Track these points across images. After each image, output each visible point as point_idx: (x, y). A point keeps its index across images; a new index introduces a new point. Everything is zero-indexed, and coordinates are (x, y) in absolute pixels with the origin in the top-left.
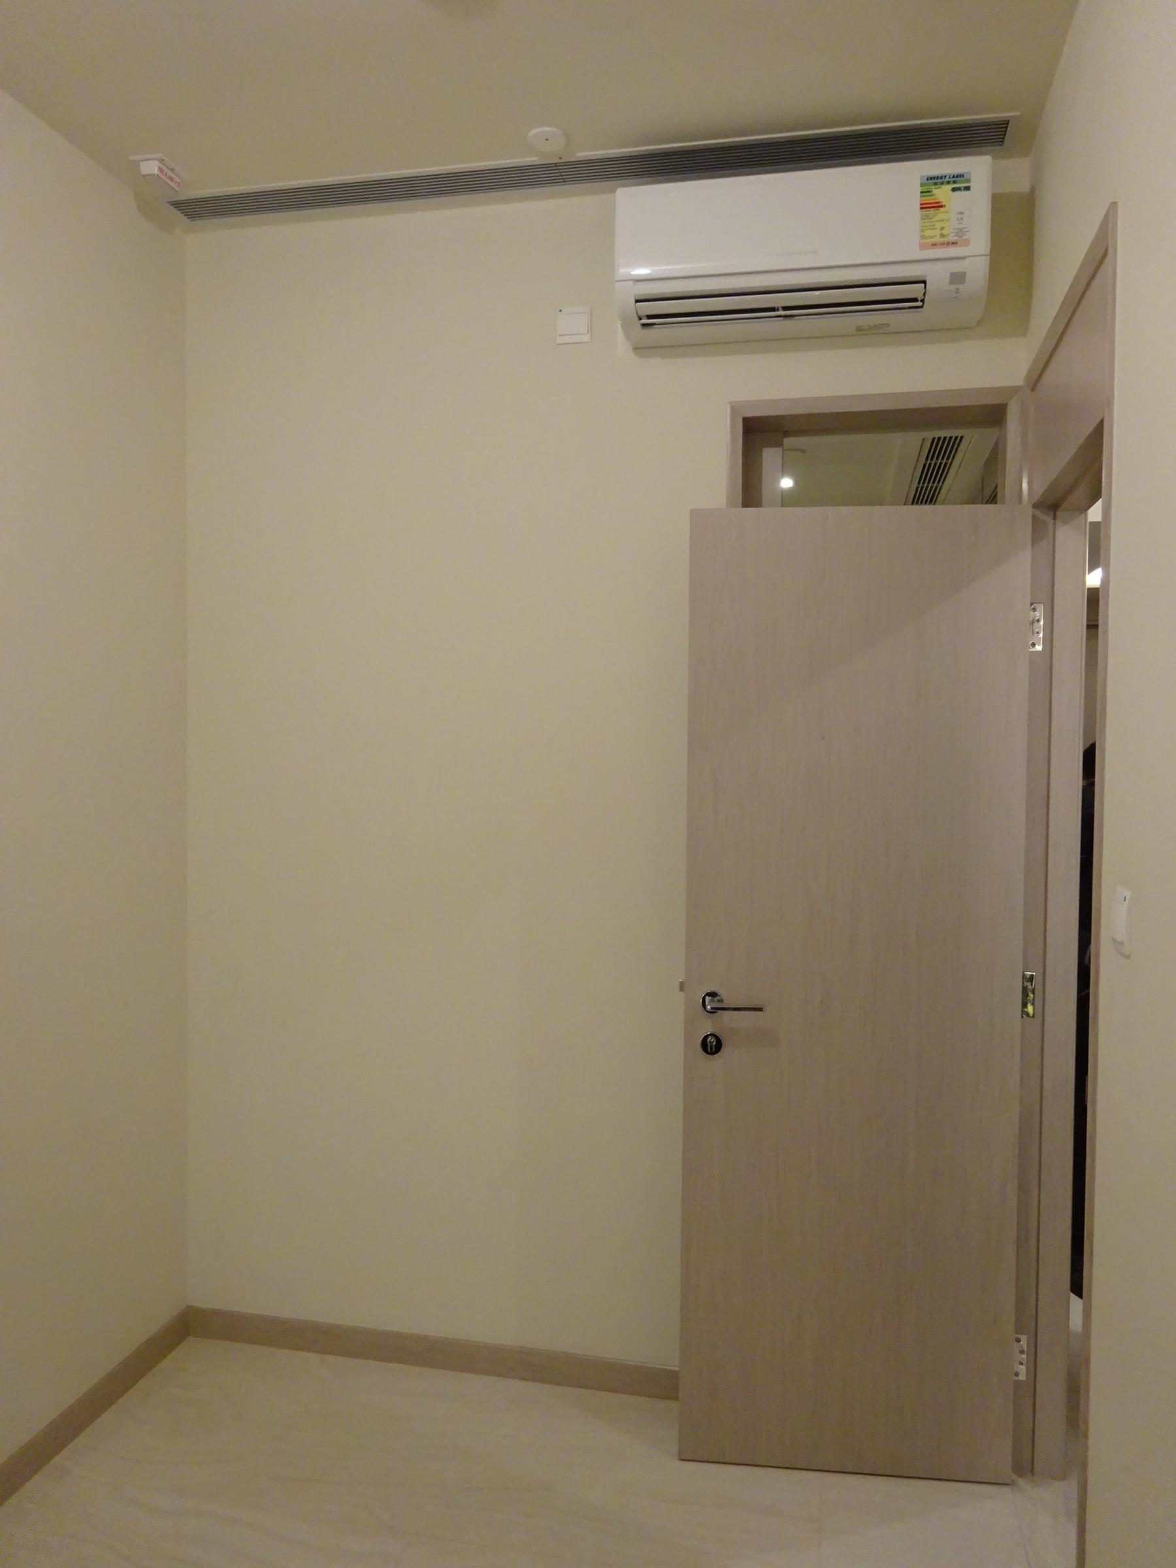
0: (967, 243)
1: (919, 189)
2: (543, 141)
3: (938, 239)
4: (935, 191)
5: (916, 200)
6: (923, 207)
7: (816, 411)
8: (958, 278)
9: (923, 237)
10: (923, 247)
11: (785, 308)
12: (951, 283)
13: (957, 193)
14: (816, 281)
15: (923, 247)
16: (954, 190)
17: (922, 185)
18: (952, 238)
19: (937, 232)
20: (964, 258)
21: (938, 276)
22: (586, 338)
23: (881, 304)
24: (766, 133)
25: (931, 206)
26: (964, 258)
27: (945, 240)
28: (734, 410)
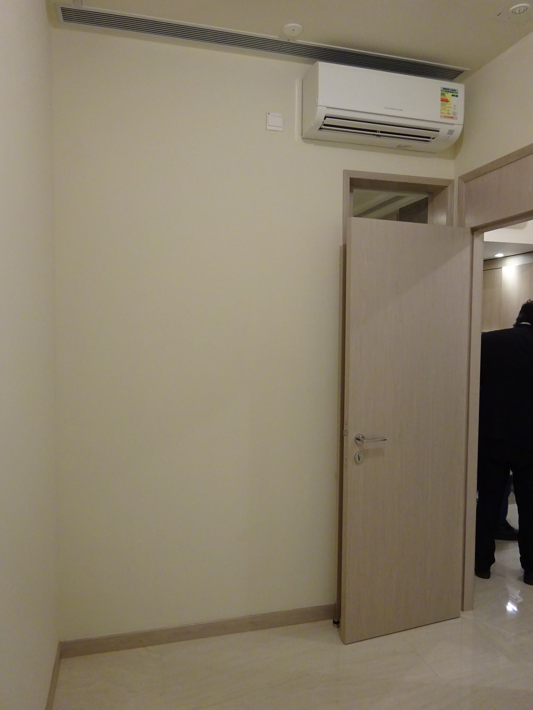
0: (456, 119)
1: (440, 92)
2: (293, 30)
3: (446, 115)
4: (446, 94)
5: (439, 97)
6: (442, 100)
7: (379, 179)
8: (451, 132)
9: (441, 113)
10: (441, 117)
11: (381, 132)
12: (448, 134)
13: (454, 97)
14: (419, 125)
15: (441, 117)
16: (453, 95)
17: (442, 91)
18: (451, 115)
19: (446, 112)
20: (454, 124)
21: (444, 129)
22: (280, 129)
23: (412, 137)
24: (388, 54)
25: (444, 100)
26: (454, 124)
27: (449, 115)
28: (346, 172)
